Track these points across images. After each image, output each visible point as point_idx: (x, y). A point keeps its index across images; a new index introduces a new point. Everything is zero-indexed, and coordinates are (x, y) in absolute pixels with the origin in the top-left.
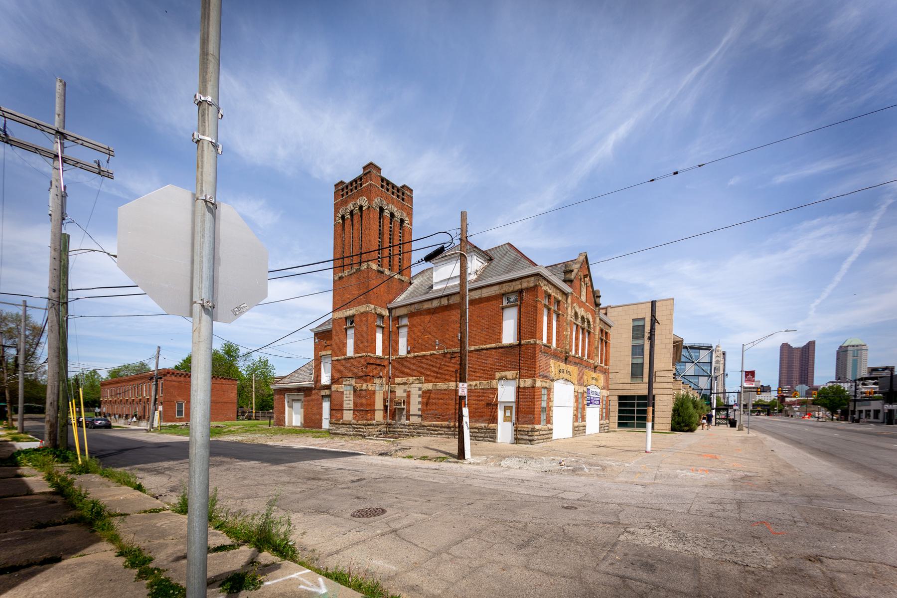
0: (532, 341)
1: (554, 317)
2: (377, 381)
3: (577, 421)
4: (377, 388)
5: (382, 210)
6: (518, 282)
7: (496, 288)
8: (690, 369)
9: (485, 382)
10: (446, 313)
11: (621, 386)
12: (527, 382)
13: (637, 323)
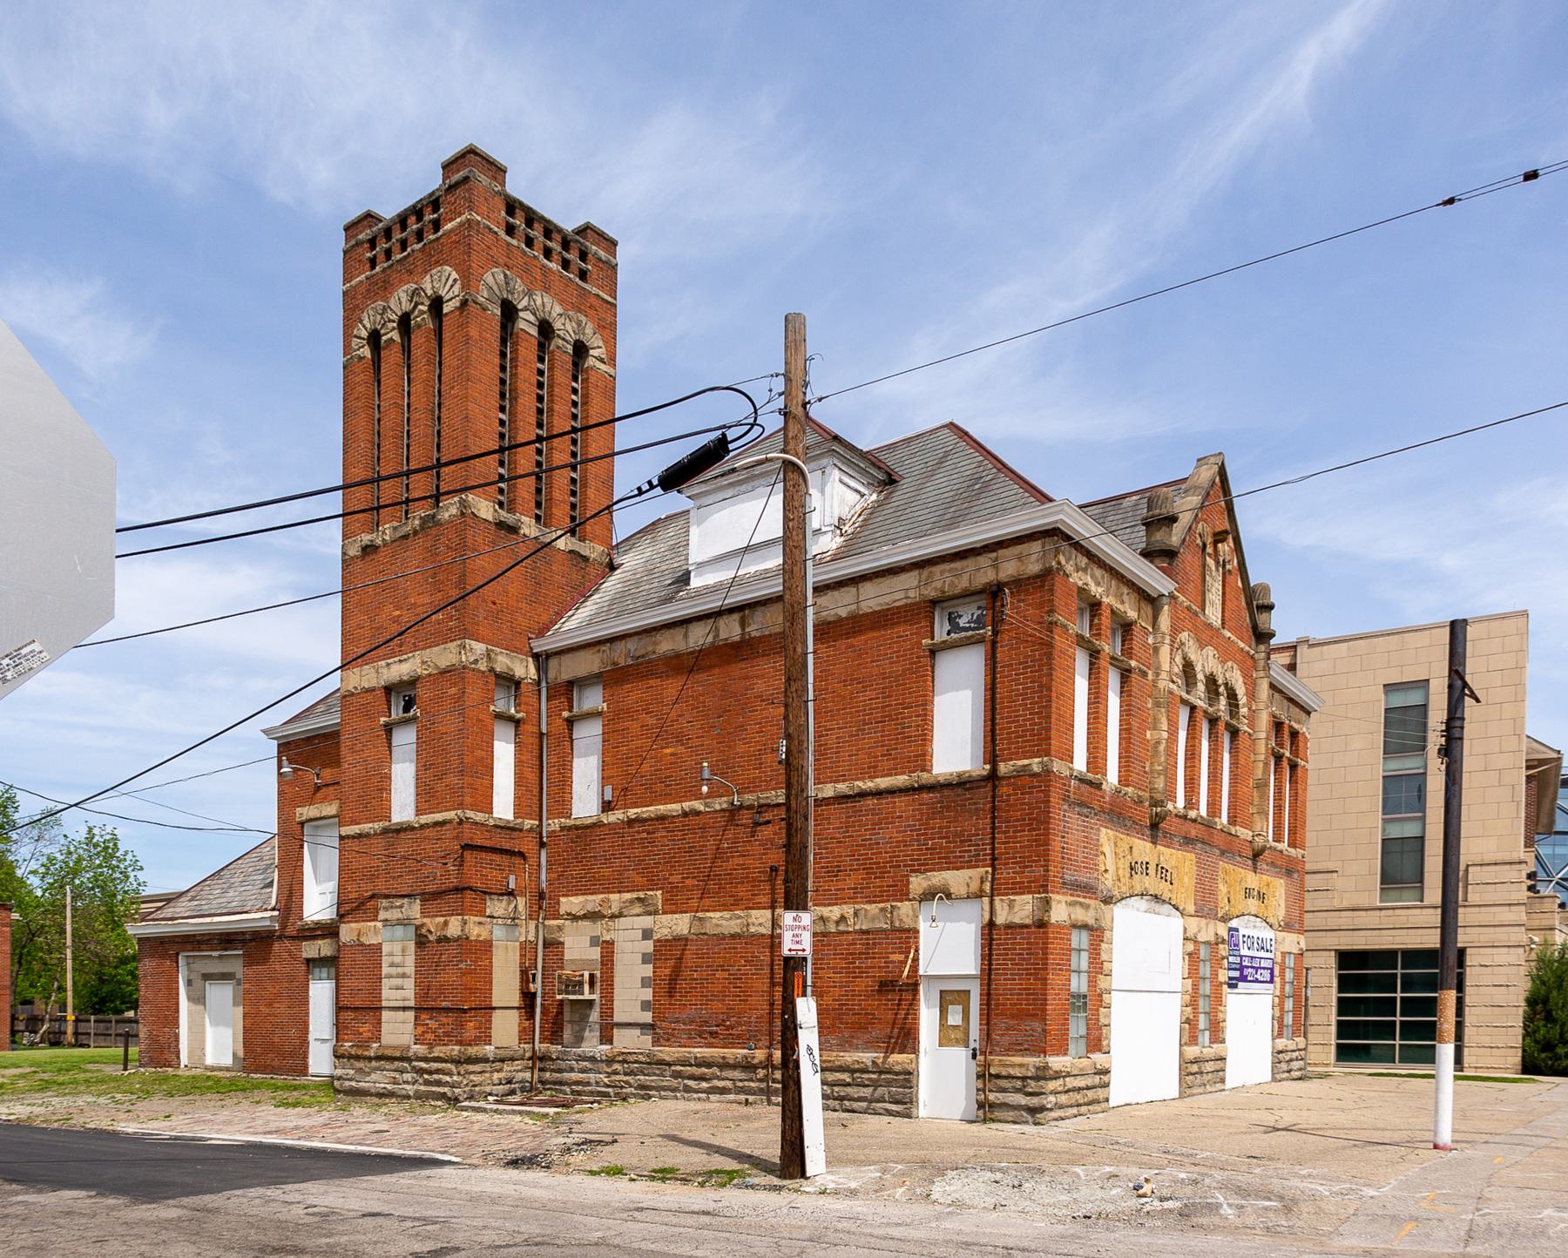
0: (1035, 764)
2: (497, 907)
3: (1193, 1040)
4: (499, 933)
5: (509, 312)
6: (985, 561)
7: (910, 579)
9: (873, 909)
10: (737, 669)
11: (1345, 920)
12: (1021, 908)
13: (1399, 700)
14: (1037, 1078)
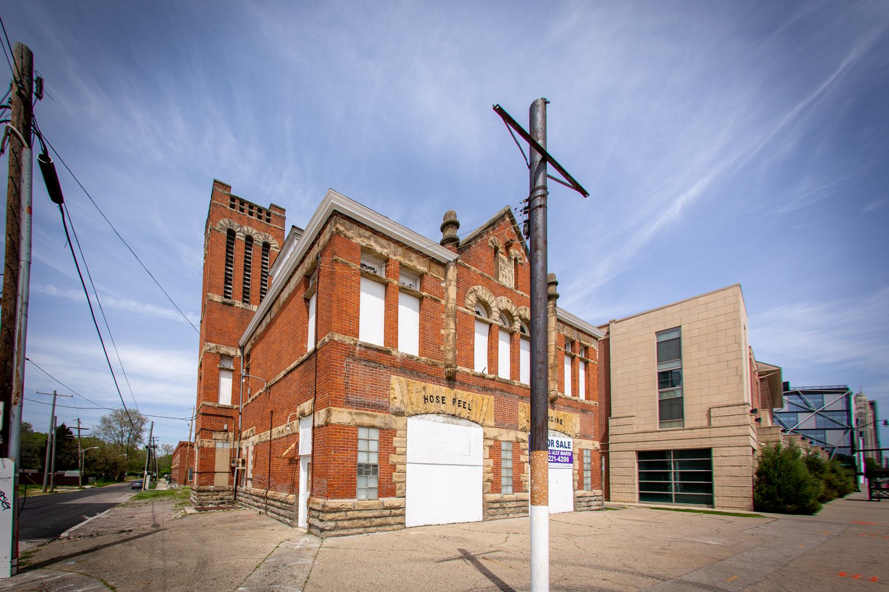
1: (581, 366)
5: (231, 233)
8: (806, 421)
11: (640, 437)
14: (322, 512)
